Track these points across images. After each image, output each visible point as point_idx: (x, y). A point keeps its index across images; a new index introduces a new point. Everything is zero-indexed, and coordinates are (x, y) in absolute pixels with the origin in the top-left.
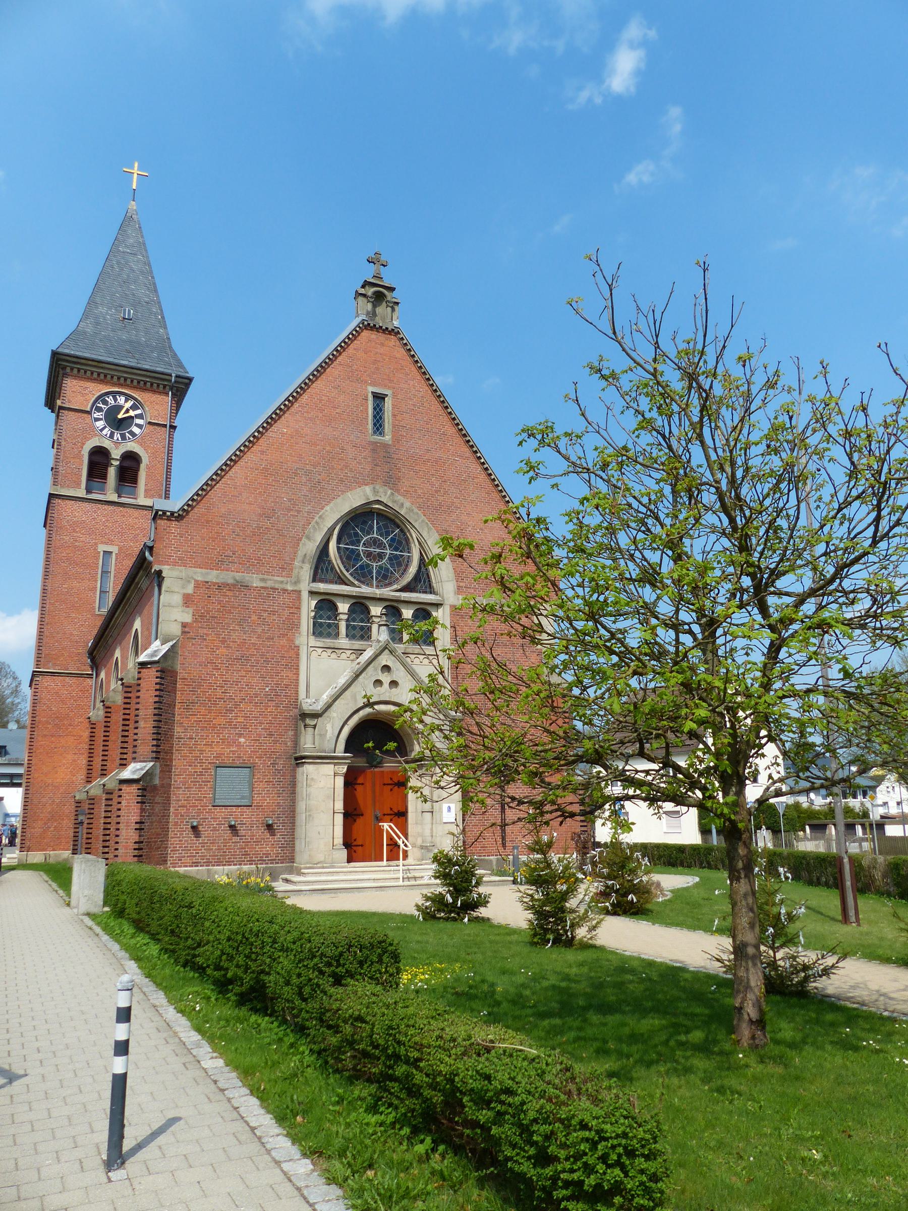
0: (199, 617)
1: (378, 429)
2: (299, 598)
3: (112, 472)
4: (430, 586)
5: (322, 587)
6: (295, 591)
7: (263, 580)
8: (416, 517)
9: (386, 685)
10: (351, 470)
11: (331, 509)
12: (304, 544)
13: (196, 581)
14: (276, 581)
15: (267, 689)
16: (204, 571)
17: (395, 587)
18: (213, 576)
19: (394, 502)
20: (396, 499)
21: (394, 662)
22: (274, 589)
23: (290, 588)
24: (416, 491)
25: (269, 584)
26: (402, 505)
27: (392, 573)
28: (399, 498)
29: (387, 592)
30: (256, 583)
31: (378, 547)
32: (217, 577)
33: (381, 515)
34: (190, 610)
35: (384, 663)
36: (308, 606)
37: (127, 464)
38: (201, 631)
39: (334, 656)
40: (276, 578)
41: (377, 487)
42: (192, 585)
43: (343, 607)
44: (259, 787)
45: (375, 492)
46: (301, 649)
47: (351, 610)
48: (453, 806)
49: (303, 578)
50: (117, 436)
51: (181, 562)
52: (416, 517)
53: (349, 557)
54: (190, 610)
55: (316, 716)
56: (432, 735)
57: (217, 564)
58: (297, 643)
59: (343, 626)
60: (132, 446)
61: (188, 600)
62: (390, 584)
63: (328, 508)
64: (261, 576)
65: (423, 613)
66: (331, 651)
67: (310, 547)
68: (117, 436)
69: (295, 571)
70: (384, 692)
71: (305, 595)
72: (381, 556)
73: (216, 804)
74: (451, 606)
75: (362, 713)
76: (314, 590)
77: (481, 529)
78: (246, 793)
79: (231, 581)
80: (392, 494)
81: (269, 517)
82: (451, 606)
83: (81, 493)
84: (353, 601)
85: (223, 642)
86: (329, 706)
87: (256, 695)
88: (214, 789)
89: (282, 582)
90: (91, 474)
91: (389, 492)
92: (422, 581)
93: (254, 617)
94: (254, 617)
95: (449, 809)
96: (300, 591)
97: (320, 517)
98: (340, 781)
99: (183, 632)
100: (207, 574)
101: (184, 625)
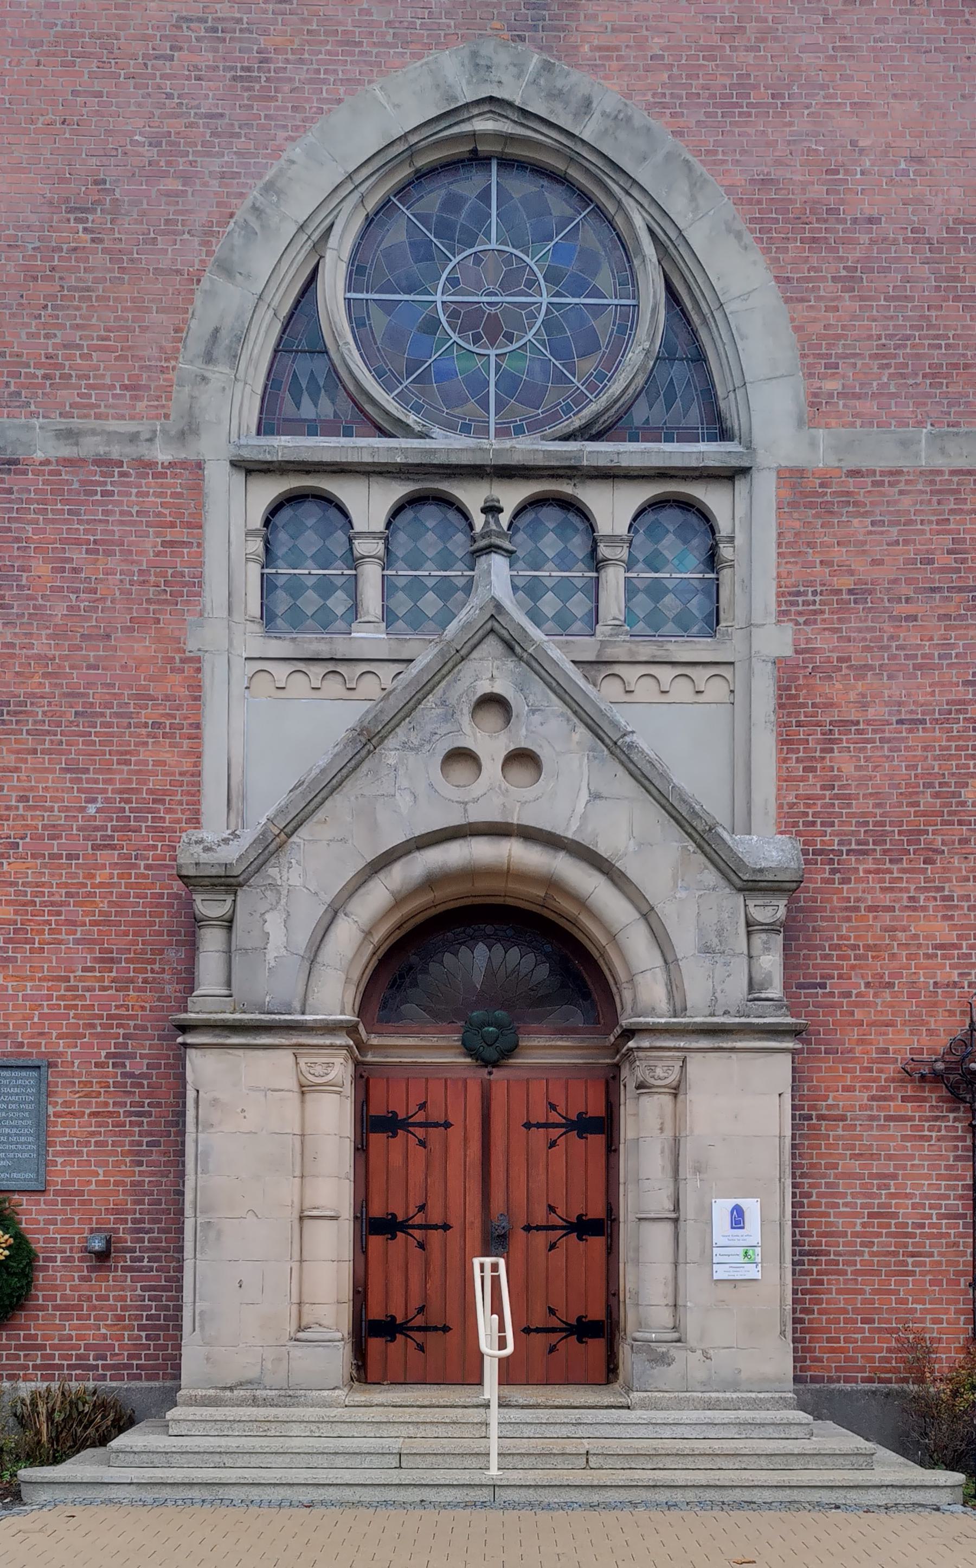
2: (197, 488)
6: (183, 464)
7: (70, 435)
12: (211, 294)
14: (111, 437)
15: (92, 809)
19: (554, 95)
20: (559, 83)
21: (521, 688)
22: (103, 462)
23: (162, 454)
24: (641, 45)
25: (91, 447)
26: (587, 103)
36: (235, 511)
40: (113, 425)
41: (487, 49)
43: (369, 505)
44: (68, 1131)
45: (479, 67)
46: (206, 667)
48: (752, 1207)
56: (678, 947)
58: (192, 645)
59: (371, 575)
63: (296, 151)
65: (676, 507)
69: (182, 395)
71: (219, 476)
76: (247, 454)
77: (917, 159)
80: (547, 67)
81: (80, 210)
89: (133, 438)
91: (535, 61)
94: (41, 568)
95: (738, 1218)
96: (200, 465)
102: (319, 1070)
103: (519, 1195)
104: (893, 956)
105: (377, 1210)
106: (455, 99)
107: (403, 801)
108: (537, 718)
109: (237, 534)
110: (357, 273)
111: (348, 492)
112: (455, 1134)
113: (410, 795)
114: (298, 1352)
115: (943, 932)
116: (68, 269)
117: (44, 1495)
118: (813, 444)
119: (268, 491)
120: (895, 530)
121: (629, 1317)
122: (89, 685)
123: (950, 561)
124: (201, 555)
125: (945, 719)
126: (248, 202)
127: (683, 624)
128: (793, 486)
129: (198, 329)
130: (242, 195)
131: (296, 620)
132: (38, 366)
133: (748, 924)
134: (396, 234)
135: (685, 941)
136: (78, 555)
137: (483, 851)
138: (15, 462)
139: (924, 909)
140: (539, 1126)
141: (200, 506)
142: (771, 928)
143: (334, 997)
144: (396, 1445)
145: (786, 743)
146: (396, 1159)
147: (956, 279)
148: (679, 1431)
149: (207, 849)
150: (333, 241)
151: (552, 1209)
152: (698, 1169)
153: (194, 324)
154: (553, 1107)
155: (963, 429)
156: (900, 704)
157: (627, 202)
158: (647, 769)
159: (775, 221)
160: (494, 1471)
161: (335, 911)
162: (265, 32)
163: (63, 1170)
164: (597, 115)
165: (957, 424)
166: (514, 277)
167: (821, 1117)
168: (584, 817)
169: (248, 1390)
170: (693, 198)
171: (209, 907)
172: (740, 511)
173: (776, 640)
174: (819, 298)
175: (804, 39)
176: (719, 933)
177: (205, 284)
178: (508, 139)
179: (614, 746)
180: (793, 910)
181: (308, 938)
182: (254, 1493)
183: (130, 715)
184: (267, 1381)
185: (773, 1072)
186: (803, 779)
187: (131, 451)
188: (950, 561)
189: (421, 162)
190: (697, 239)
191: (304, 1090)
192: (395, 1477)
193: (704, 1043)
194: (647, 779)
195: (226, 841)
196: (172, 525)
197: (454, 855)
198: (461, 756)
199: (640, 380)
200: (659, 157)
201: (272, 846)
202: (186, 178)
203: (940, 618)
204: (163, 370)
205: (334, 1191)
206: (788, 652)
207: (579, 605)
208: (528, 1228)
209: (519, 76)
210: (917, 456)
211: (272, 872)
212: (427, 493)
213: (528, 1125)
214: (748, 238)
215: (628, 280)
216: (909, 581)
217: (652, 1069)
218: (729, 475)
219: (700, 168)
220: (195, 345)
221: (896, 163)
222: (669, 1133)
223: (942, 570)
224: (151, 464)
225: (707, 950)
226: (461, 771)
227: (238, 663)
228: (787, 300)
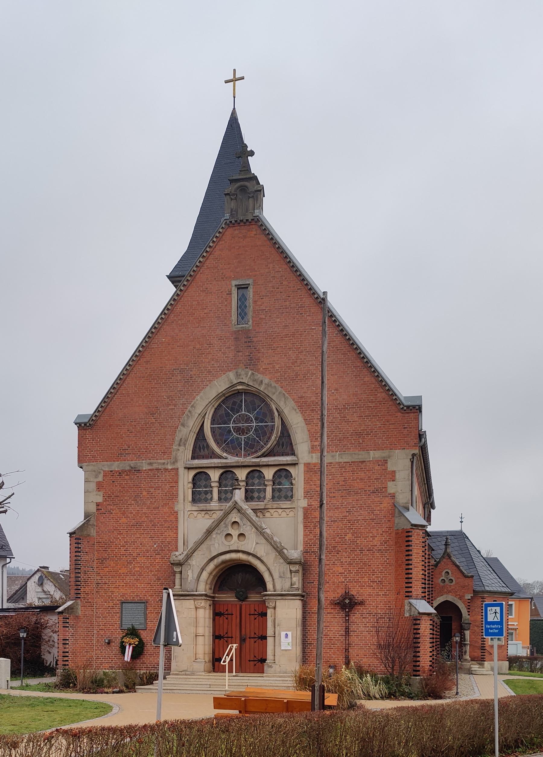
1: (243, 318)
2: (177, 474)
4: (292, 449)
5: (197, 462)
6: (174, 469)
7: (150, 464)
8: (274, 390)
9: (235, 537)
10: (217, 361)
11: (201, 398)
12: (180, 431)
13: (104, 471)
15: (155, 546)
16: (109, 463)
17: (260, 454)
18: (116, 466)
19: (254, 380)
20: (256, 377)
21: (241, 520)
23: (170, 467)
24: (274, 367)
25: (155, 466)
26: (262, 381)
27: (258, 442)
28: (260, 377)
29: (251, 460)
30: (146, 467)
31: (246, 422)
32: (118, 467)
33: (246, 393)
34: (101, 493)
35: (234, 520)
36: (185, 479)
38: (109, 507)
39: (207, 516)
40: (159, 461)
41: (240, 371)
42: (101, 475)
43: (215, 475)
45: (238, 375)
46: (179, 514)
48: (289, 634)
49: (180, 458)
52: (274, 390)
54: (101, 493)
55: (180, 564)
58: (176, 509)
62: (256, 452)
63: (198, 398)
64: (148, 461)
65: (283, 473)
66: (204, 513)
69: (174, 454)
70: (234, 543)
71: (181, 471)
72: (249, 429)
73: (122, 628)
74: (305, 464)
78: (143, 621)
79: (128, 468)
80: (253, 374)
82: (305, 464)
84: (221, 471)
85: (124, 514)
86: (189, 557)
87: (148, 551)
89: (164, 464)
91: (250, 372)
93: (145, 493)
94: (145, 493)
96: (178, 469)
97: (192, 406)
99: (97, 509)
100: (112, 465)
101: (98, 505)
102: (199, 604)
103: (248, 631)
104: (329, 576)
105: (217, 634)
106: (232, 383)
107: (216, 545)
108: (244, 526)
109: (186, 484)
110: (213, 422)
111: (211, 472)
112: (234, 616)
113: (218, 544)
114: (195, 664)
115: (341, 570)
116: (151, 427)
117: (140, 691)
118: (312, 457)
120: (330, 476)
122: (154, 519)
123: (343, 483)
124: (178, 489)
125: (342, 520)
126: (188, 410)
128: (307, 467)
129: (177, 439)
130: (187, 408)
132: (144, 449)
133: (291, 571)
134: (222, 412)
135: (276, 575)
136: (152, 490)
138: (139, 470)
139: (337, 564)
140: (252, 615)
141: (178, 478)
142: (297, 572)
143: (203, 588)
144: (209, 683)
145: (305, 527)
146: (221, 622)
147: (345, 417)
148: (270, 682)
149: (176, 557)
150: (207, 416)
151: (255, 634)
152: (278, 625)
153: (176, 438)
154: (255, 610)
155: (346, 452)
156: (331, 517)
157: (271, 403)
158: (267, 537)
159: (303, 406)
160: (227, 688)
161: (203, 569)
162: (192, 371)
164: (264, 384)
165: (345, 451)
166: (248, 420)
167: (312, 613)
168: (255, 548)
169: (184, 672)
170: (285, 402)
171: (177, 569)
172: (297, 473)
174: (314, 423)
175: (310, 363)
176: (283, 574)
177: (179, 429)
178: (245, 389)
179: (260, 531)
180: (304, 566)
181: (198, 575)
182: (179, 691)
183: (163, 525)
184: (189, 670)
185: (297, 604)
186: (309, 535)
187: (163, 467)
188: (343, 483)
189: (226, 396)
190: (286, 411)
191: (196, 608)
192: (209, 689)
193: (279, 598)
194: (268, 539)
195: (180, 555)
196: (172, 482)
198: (229, 535)
199: (275, 443)
200: (277, 393)
202: (175, 405)
203: (341, 497)
204: (170, 448)
206: (306, 506)
208: (250, 638)
209: (247, 377)
210: (336, 459)
211: (189, 561)
213: (250, 615)
214: (298, 410)
216: (334, 488)
217: (269, 603)
218: (294, 464)
219: (287, 395)
220: (177, 443)
221: (331, 391)
222: (273, 618)
223: (341, 485)
224: (167, 469)
225: (281, 577)
226: (229, 538)
227: (186, 512)
228: (306, 424)
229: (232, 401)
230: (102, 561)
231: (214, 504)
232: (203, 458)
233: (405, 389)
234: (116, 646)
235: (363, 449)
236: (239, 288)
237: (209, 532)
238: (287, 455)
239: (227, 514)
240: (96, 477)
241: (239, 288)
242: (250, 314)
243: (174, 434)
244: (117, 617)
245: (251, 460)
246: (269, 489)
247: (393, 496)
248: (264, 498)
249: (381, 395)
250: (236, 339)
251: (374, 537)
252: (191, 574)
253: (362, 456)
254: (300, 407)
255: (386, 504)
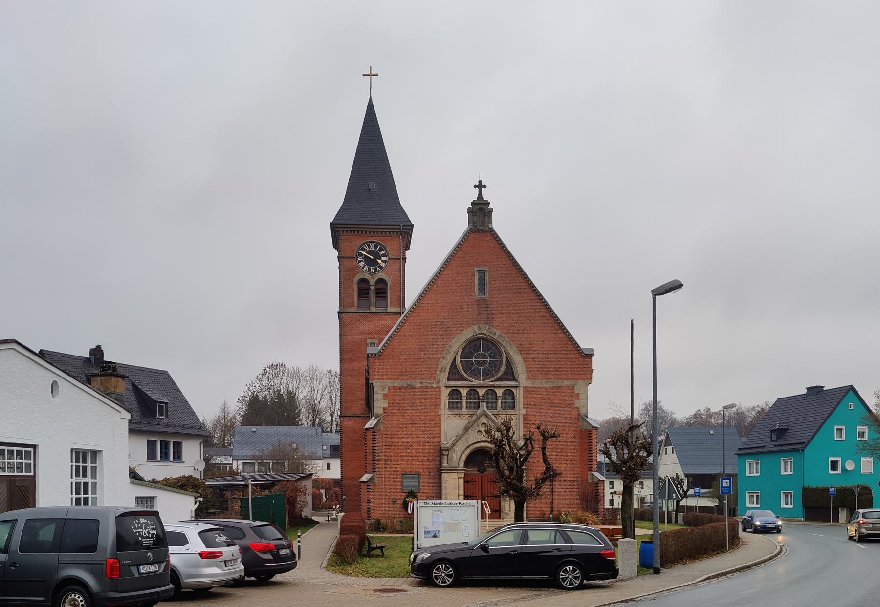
0: (391, 404)
2: (440, 390)
3: (372, 294)
5: (452, 383)
18: (397, 384)
23: (435, 386)
25: (424, 385)
28: (494, 330)
29: (487, 382)
30: (418, 385)
33: (483, 339)
36: (445, 393)
37: (379, 286)
43: (464, 392)
45: (479, 328)
47: (469, 394)
50: (372, 270)
51: (382, 378)
53: (468, 367)
55: (448, 450)
57: (399, 377)
60: (381, 275)
61: (385, 397)
62: (490, 378)
65: (509, 392)
67: (447, 363)
68: (372, 270)
71: (443, 388)
72: (484, 363)
75: (483, 444)
83: (355, 309)
86: (454, 445)
88: (402, 485)
90: (359, 296)
92: (510, 374)
98: (462, 481)
101: (384, 409)
111: (461, 390)
119: (449, 390)
121: (503, 509)
127: (510, 408)
129: (440, 367)
131: (453, 408)
137: (483, 444)
143: (462, 464)
159: (522, 350)
163: (422, 489)
166: (484, 357)
171: (445, 453)
173: (523, 412)
181: (458, 456)
197: (479, 445)
201: (454, 445)
205: (462, 492)
207: (494, 405)
212: (473, 390)
215: (501, 358)
220: (439, 369)
229: (473, 345)
230: (388, 447)
231: (464, 411)
232: (455, 380)
233: (583, 344)
234: (399, 504)
235: (559, 379)
236: (479, 272)
237: (467, 429)
238: (510, 380)
239: (478, 418)
240: (383, 390)
241: (479, 272)
242: (487, 290)
243: (437, 364)
244: (399, 484)
245: (487, 382)
246: (499, 402)
247: (578, 409)
248: (496, 407)
249: (570, 346)
250: (478, 305)
251: (567, 434)
252: (455, 456)
253: (559, 383)
254: (520, 351)
255: (574, 413)
